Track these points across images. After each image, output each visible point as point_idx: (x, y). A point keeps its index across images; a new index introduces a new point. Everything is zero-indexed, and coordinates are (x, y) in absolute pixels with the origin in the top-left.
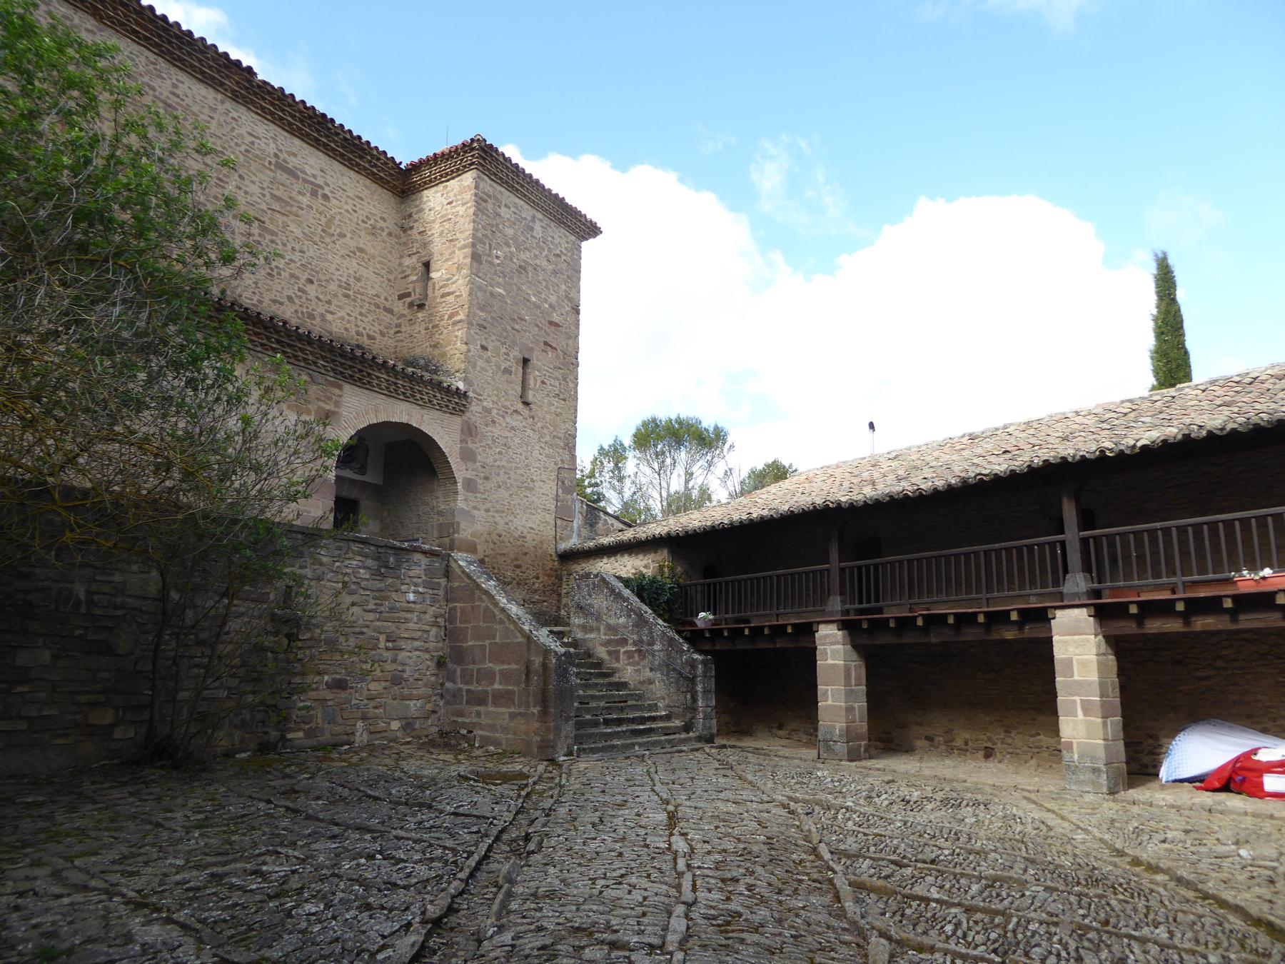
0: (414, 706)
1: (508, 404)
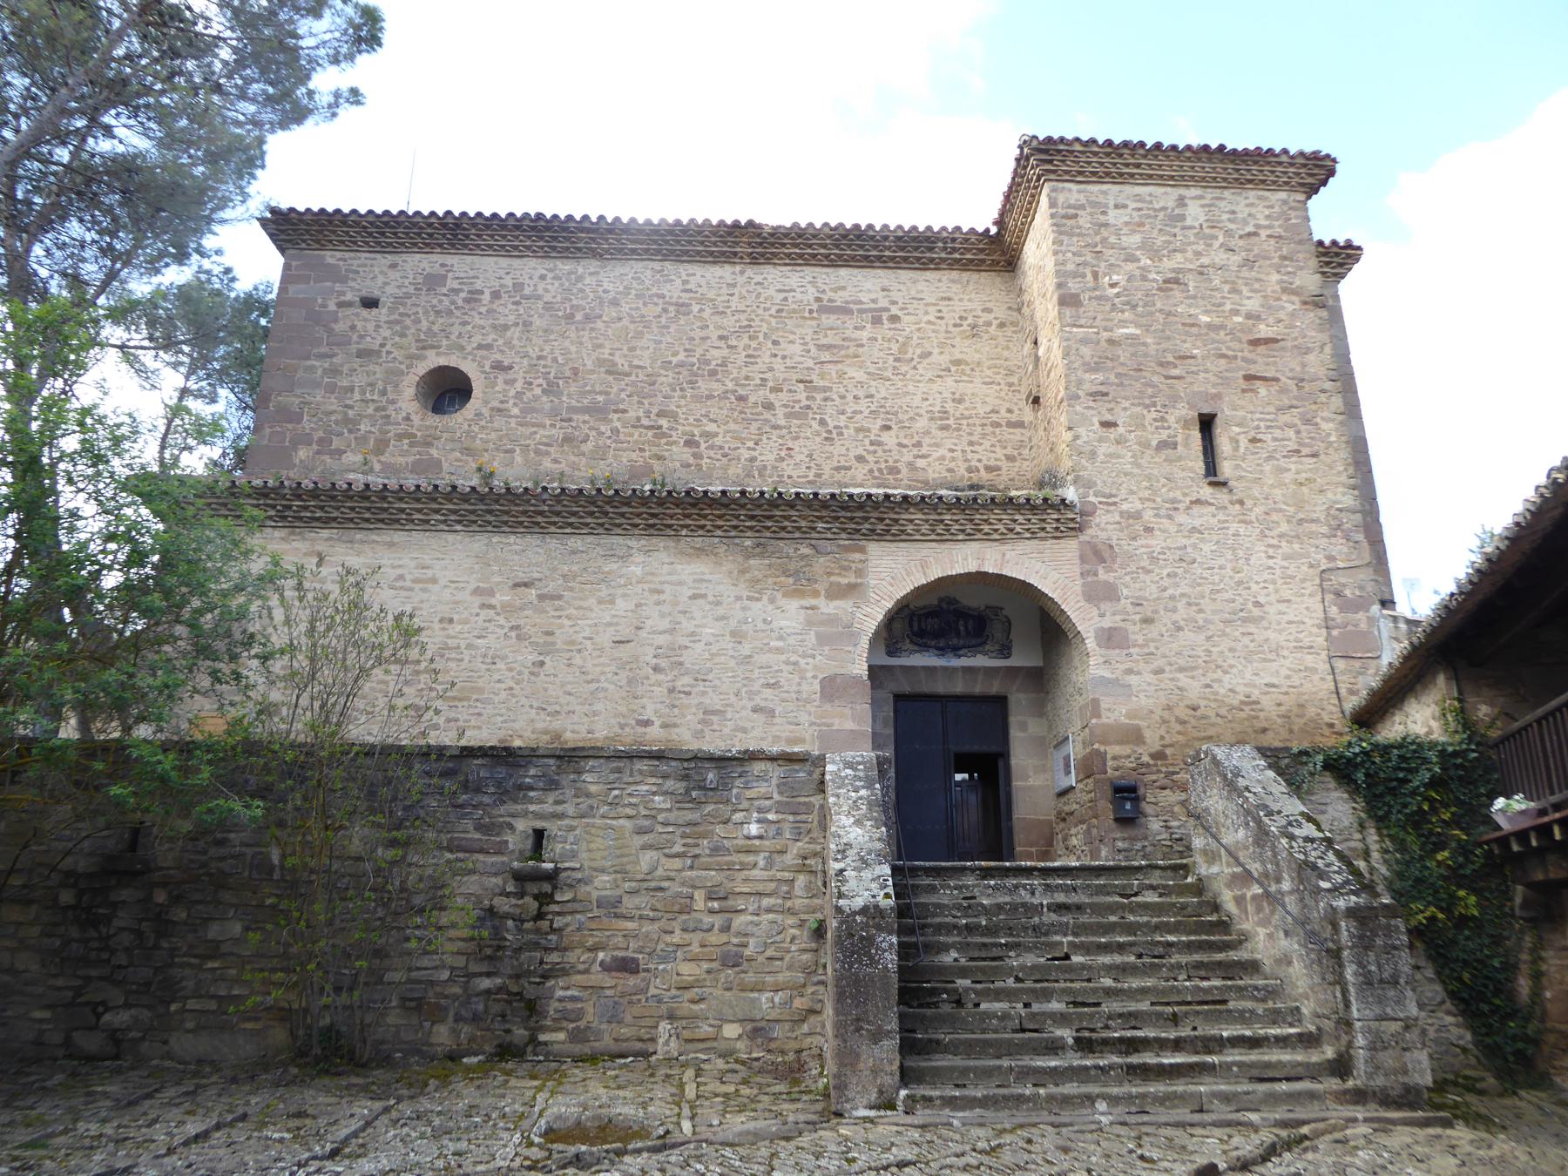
0: (766, 1003)
1: (1178, 494)
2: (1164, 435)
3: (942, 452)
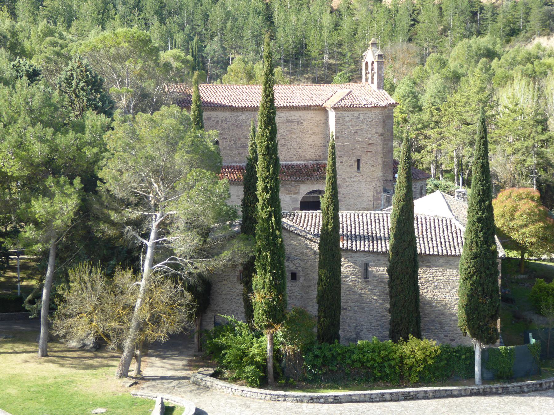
2: (351, 164)
3: (310, 153)
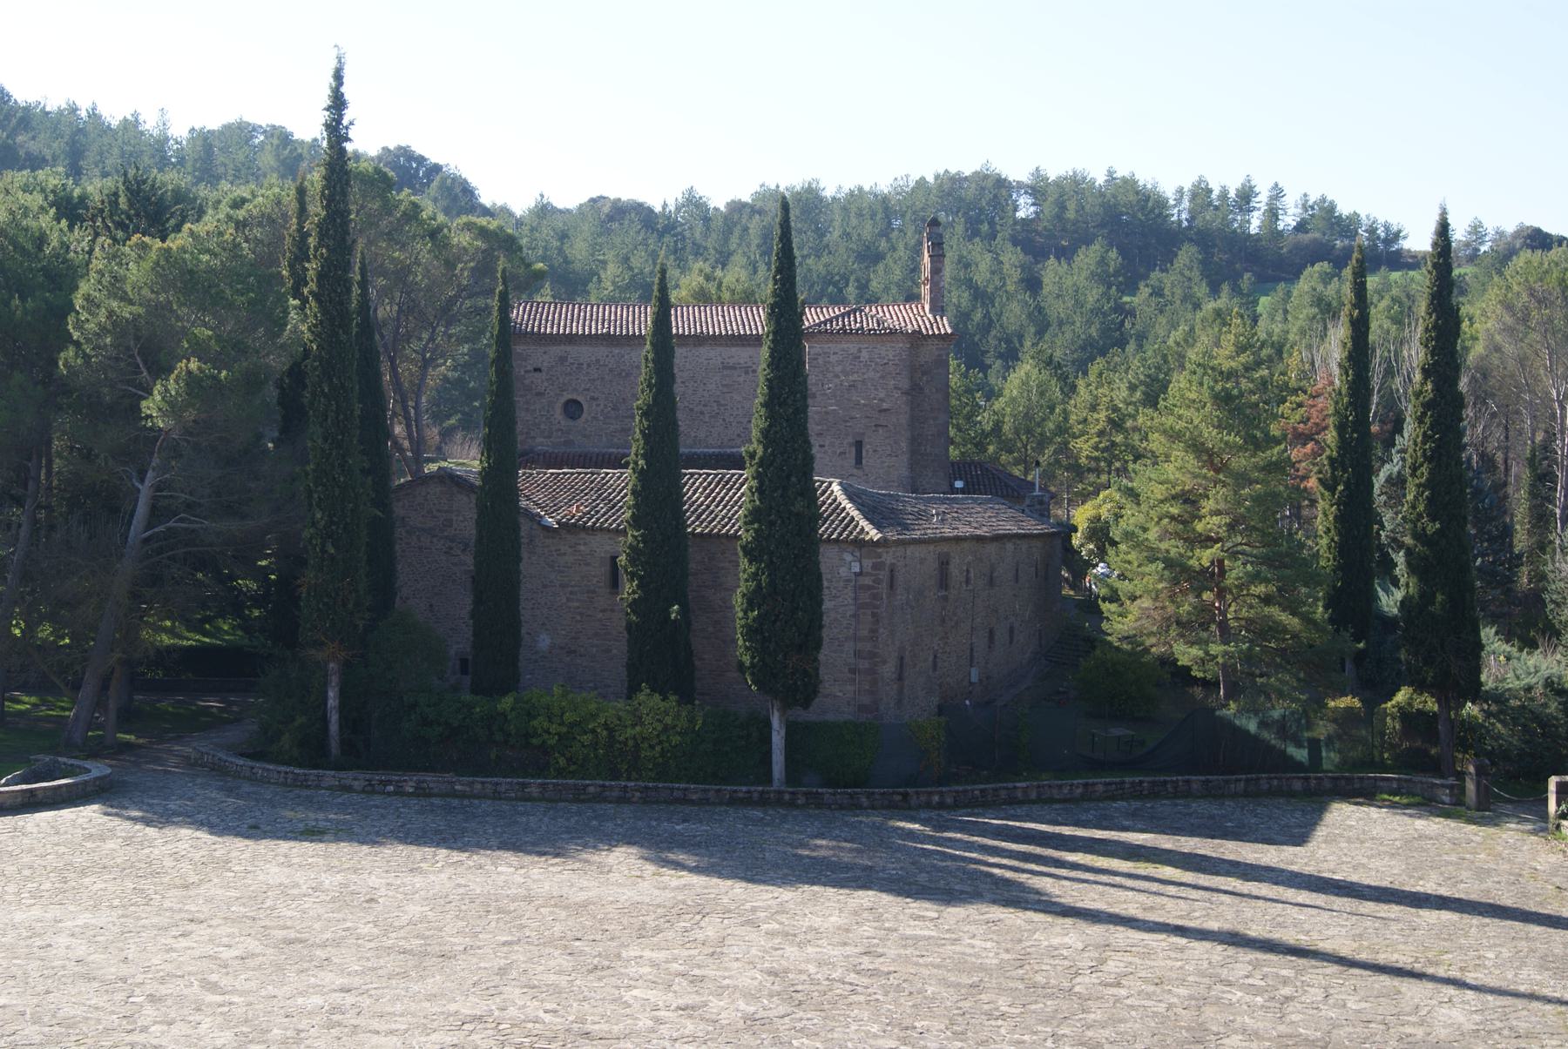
2: (842, 450)
